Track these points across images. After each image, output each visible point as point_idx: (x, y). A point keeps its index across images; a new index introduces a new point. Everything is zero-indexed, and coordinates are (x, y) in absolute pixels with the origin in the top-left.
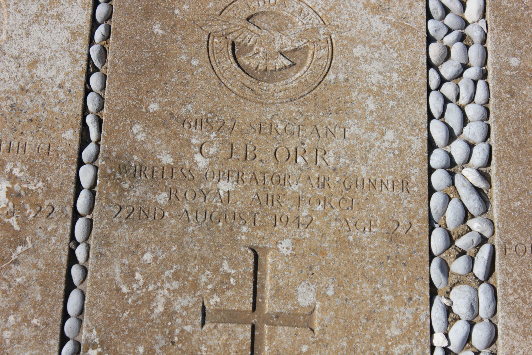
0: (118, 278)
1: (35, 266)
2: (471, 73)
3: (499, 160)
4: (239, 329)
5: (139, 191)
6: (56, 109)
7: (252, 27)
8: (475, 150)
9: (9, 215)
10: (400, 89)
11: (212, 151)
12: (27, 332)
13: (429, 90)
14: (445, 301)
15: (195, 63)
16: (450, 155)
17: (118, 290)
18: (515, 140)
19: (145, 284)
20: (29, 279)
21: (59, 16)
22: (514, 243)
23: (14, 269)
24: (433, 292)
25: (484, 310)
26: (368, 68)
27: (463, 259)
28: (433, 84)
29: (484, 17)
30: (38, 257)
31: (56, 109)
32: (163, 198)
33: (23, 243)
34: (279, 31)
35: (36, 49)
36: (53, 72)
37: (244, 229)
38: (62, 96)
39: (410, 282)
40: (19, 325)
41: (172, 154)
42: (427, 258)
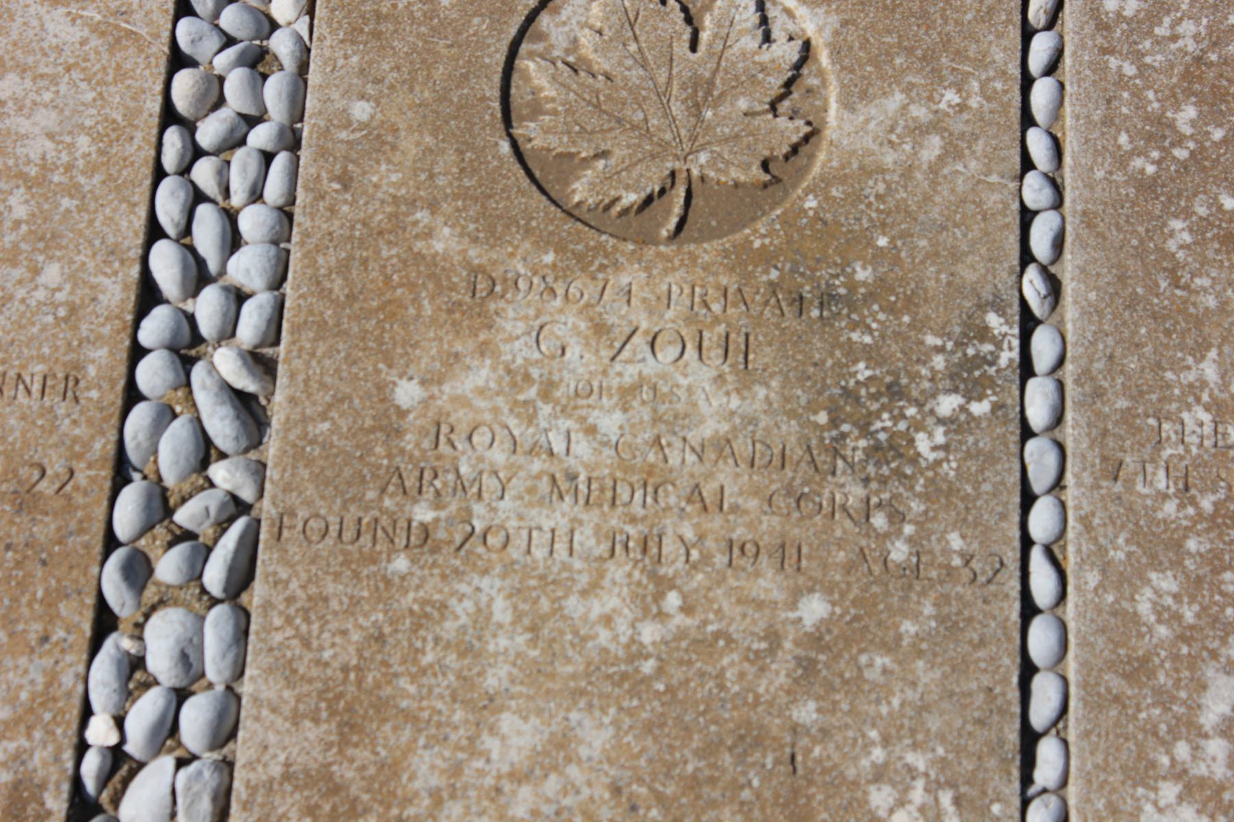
2: (260, 137)
3: (296, 329)
8: (248, 308)
10: (91, 171)
13: (159, 174)
14: (128, 644)
16: (191, 319)
18: (337, 286)
22: (302, 513)
24: (105, 622)
25: (215, 666)
26: (22, 124)
27: (181, 549)
28: (170, 160)
29: (311, 12)
39: (50, 602)
42: (98, 548)
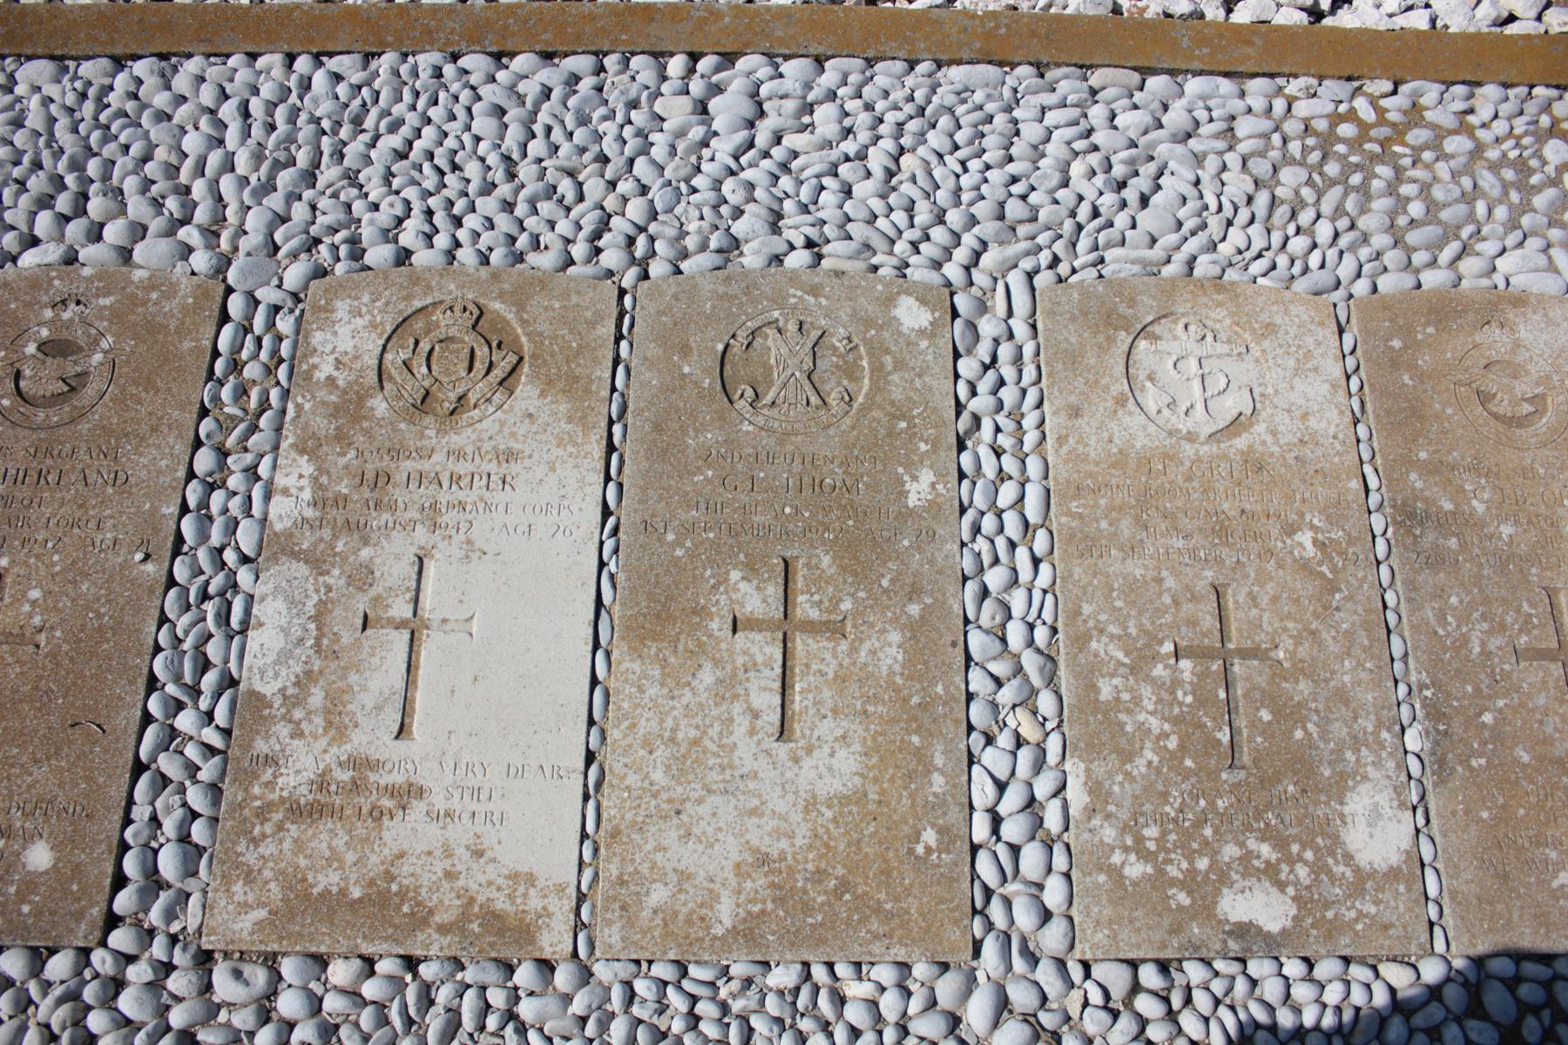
0: (1432, 621)
1: (1355, 612)
4: (1552, 666)
5: (1430, 537)
6: (1336, 460)
7: (1491, 376)
9: (1320, 563)
11: (1486, 496)
12: (1363, 675)
15: (1449, 411)
17: (1436, 633)
19: (1458, 626)
20: (1353, 625)
21: (1316, 369)
23: (1338, 616)
30: (1356, 603)
31: (1336, 460)
32: (1453, 543)
33: (1339, 590)
34: (1515, 378)
35: (1302, 402)
36: (1324, 424)
37: (1534, 570)
38: (1338, 447)
40: (1355, 669)
41: (1451, 500)
